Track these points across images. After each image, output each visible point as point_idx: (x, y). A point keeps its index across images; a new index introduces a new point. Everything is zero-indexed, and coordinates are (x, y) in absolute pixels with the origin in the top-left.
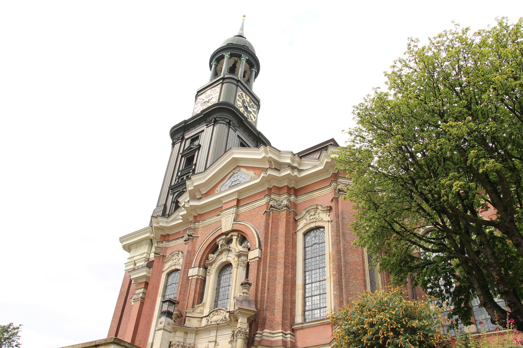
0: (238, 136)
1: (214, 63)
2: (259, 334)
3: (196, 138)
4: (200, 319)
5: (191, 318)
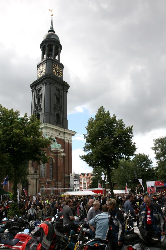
0: (55, 87)
3: (40, 90)
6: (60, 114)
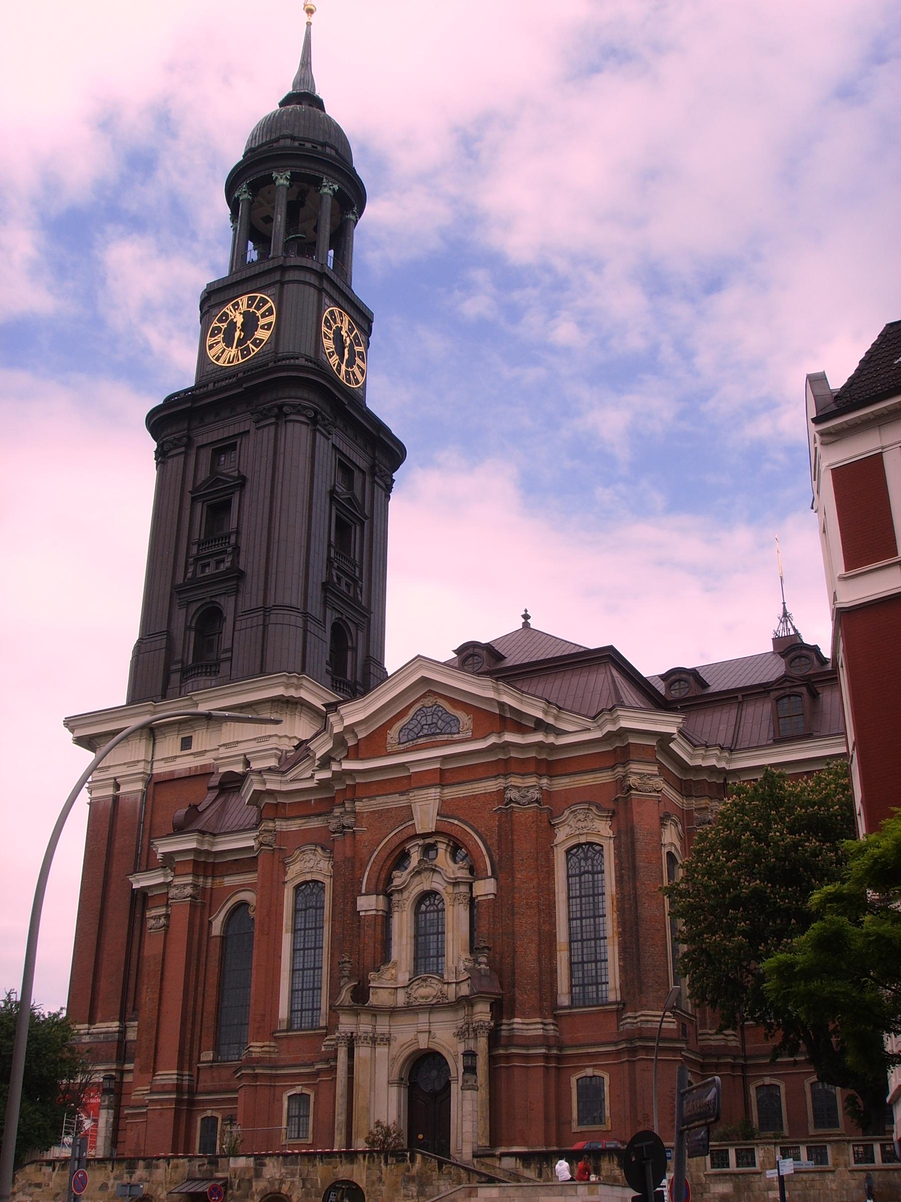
0: (333, 446)
1: (243, 194)
2: (505, 1024)
4: (393, 990)
5: (378, 990)
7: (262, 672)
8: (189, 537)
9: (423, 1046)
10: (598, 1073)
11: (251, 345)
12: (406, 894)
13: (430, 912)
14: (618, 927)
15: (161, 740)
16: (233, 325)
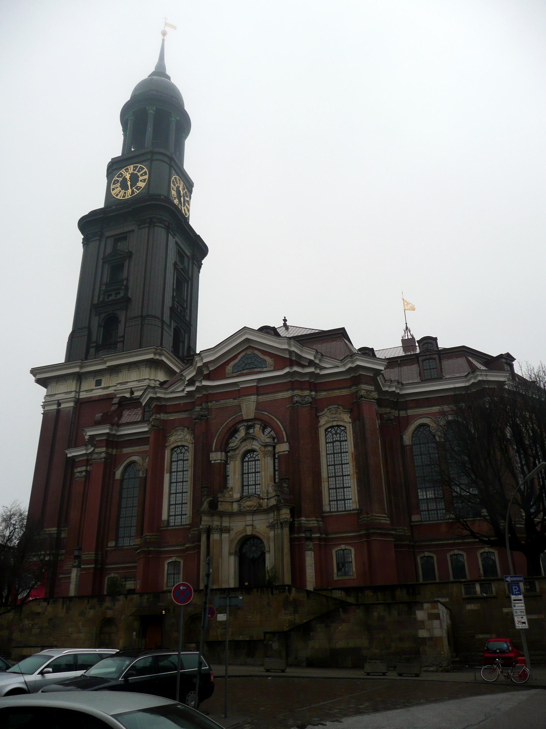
0: (176, 243)
5: (223, 503)
6: (182, 330)
7: (140, 347)
8: (101, 281)
9: (249, 533)
10: (348, 547)
11: (135, 189)
12: (237, 452)
13: (251, 461)
14: (356, 470)
15: (85, 381)
16: (125, 179)
